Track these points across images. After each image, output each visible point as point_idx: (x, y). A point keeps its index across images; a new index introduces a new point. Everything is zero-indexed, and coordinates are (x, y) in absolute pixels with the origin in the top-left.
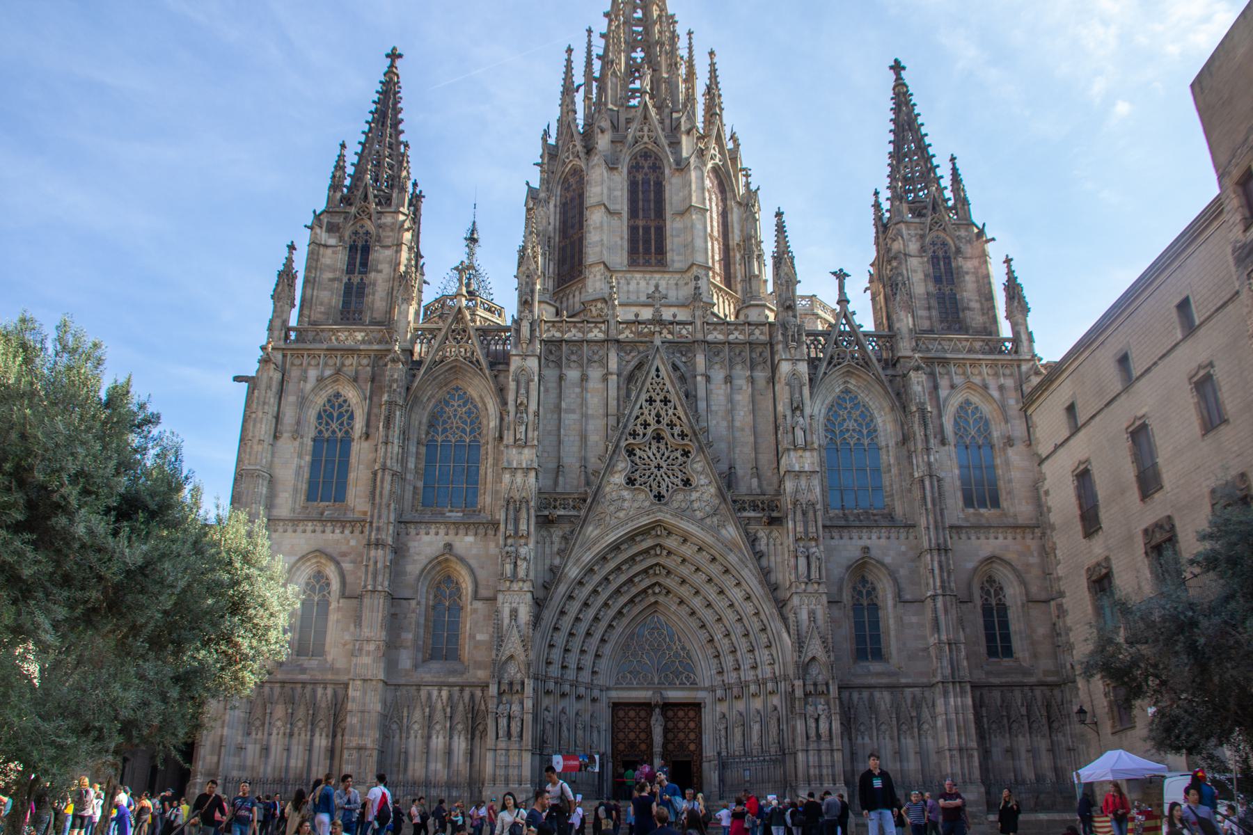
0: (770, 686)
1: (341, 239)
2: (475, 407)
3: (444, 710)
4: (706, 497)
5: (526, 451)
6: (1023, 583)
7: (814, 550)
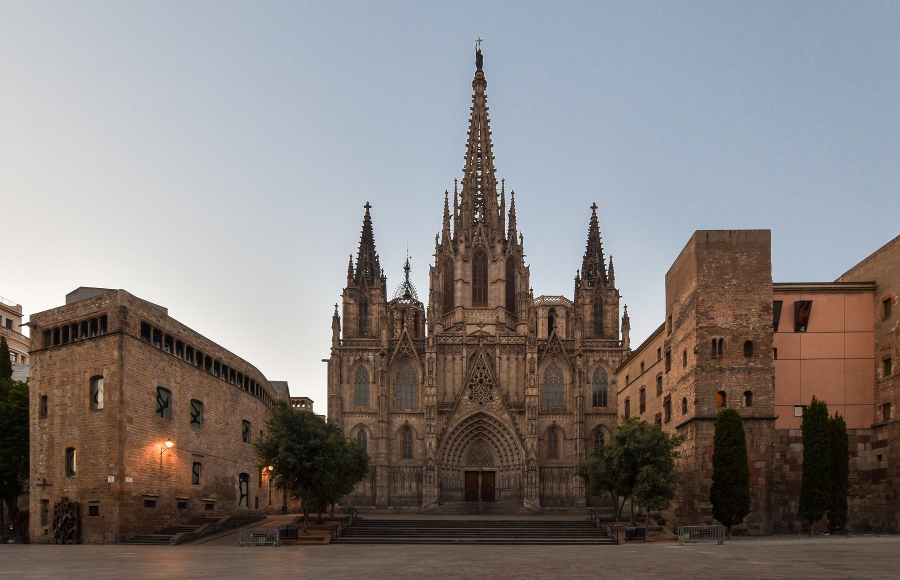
1: (355, 300)
6: (611, 434)
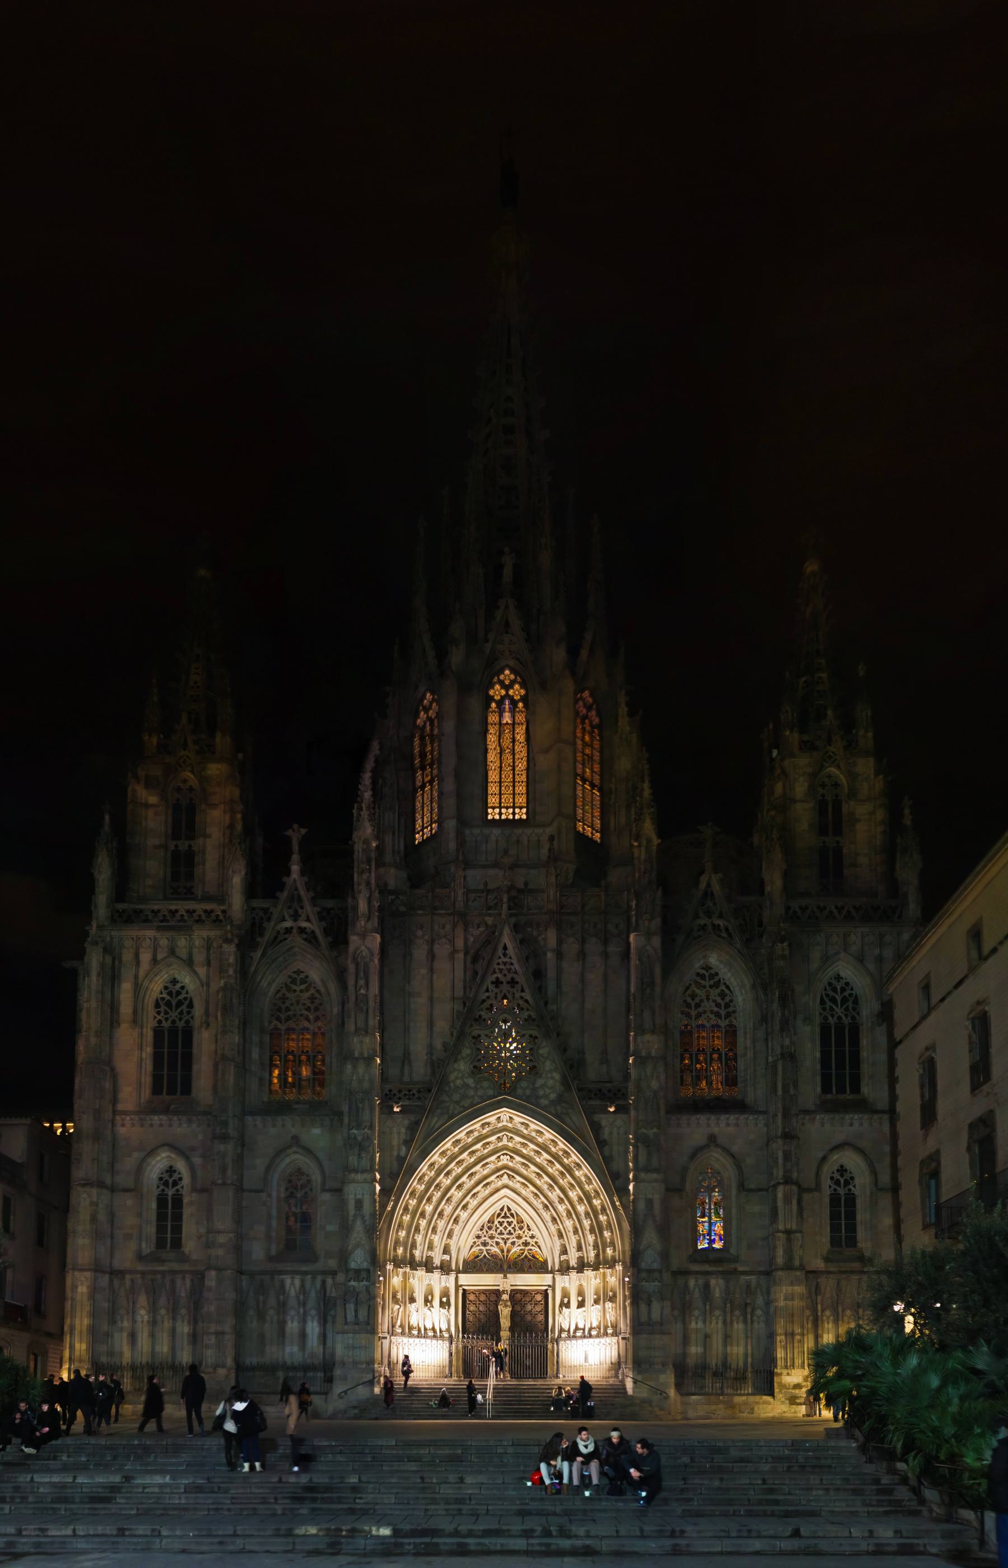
2: (318, 991)
6: (874, 1173)
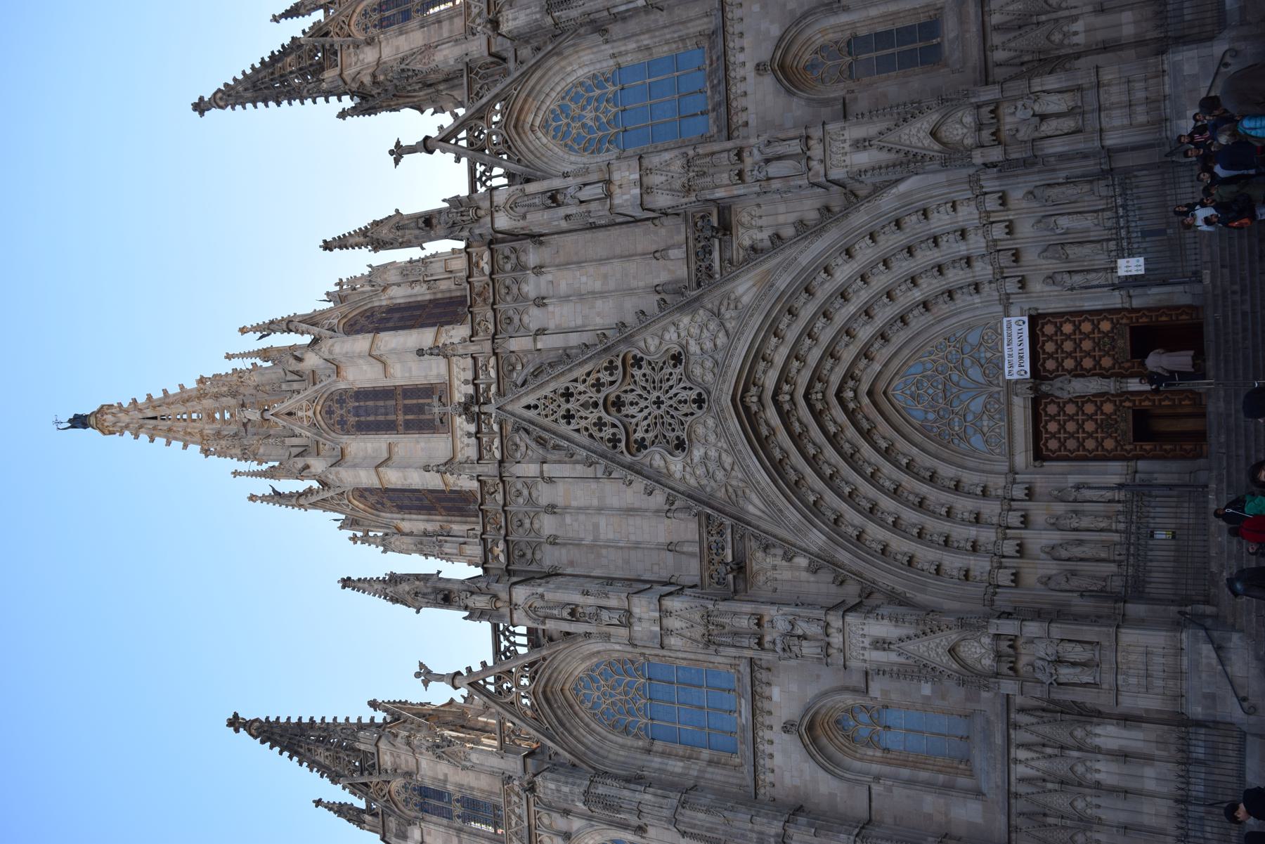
0: (991, 203)
1: (410, 823)
2: (597, 666)
3: (1050, 756)
4: (695, 331)
5: (636, 611)
7: (755, 151)
